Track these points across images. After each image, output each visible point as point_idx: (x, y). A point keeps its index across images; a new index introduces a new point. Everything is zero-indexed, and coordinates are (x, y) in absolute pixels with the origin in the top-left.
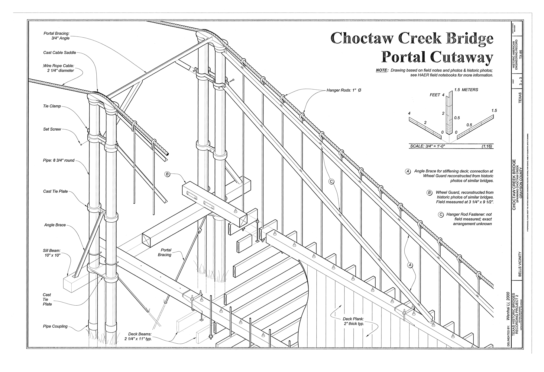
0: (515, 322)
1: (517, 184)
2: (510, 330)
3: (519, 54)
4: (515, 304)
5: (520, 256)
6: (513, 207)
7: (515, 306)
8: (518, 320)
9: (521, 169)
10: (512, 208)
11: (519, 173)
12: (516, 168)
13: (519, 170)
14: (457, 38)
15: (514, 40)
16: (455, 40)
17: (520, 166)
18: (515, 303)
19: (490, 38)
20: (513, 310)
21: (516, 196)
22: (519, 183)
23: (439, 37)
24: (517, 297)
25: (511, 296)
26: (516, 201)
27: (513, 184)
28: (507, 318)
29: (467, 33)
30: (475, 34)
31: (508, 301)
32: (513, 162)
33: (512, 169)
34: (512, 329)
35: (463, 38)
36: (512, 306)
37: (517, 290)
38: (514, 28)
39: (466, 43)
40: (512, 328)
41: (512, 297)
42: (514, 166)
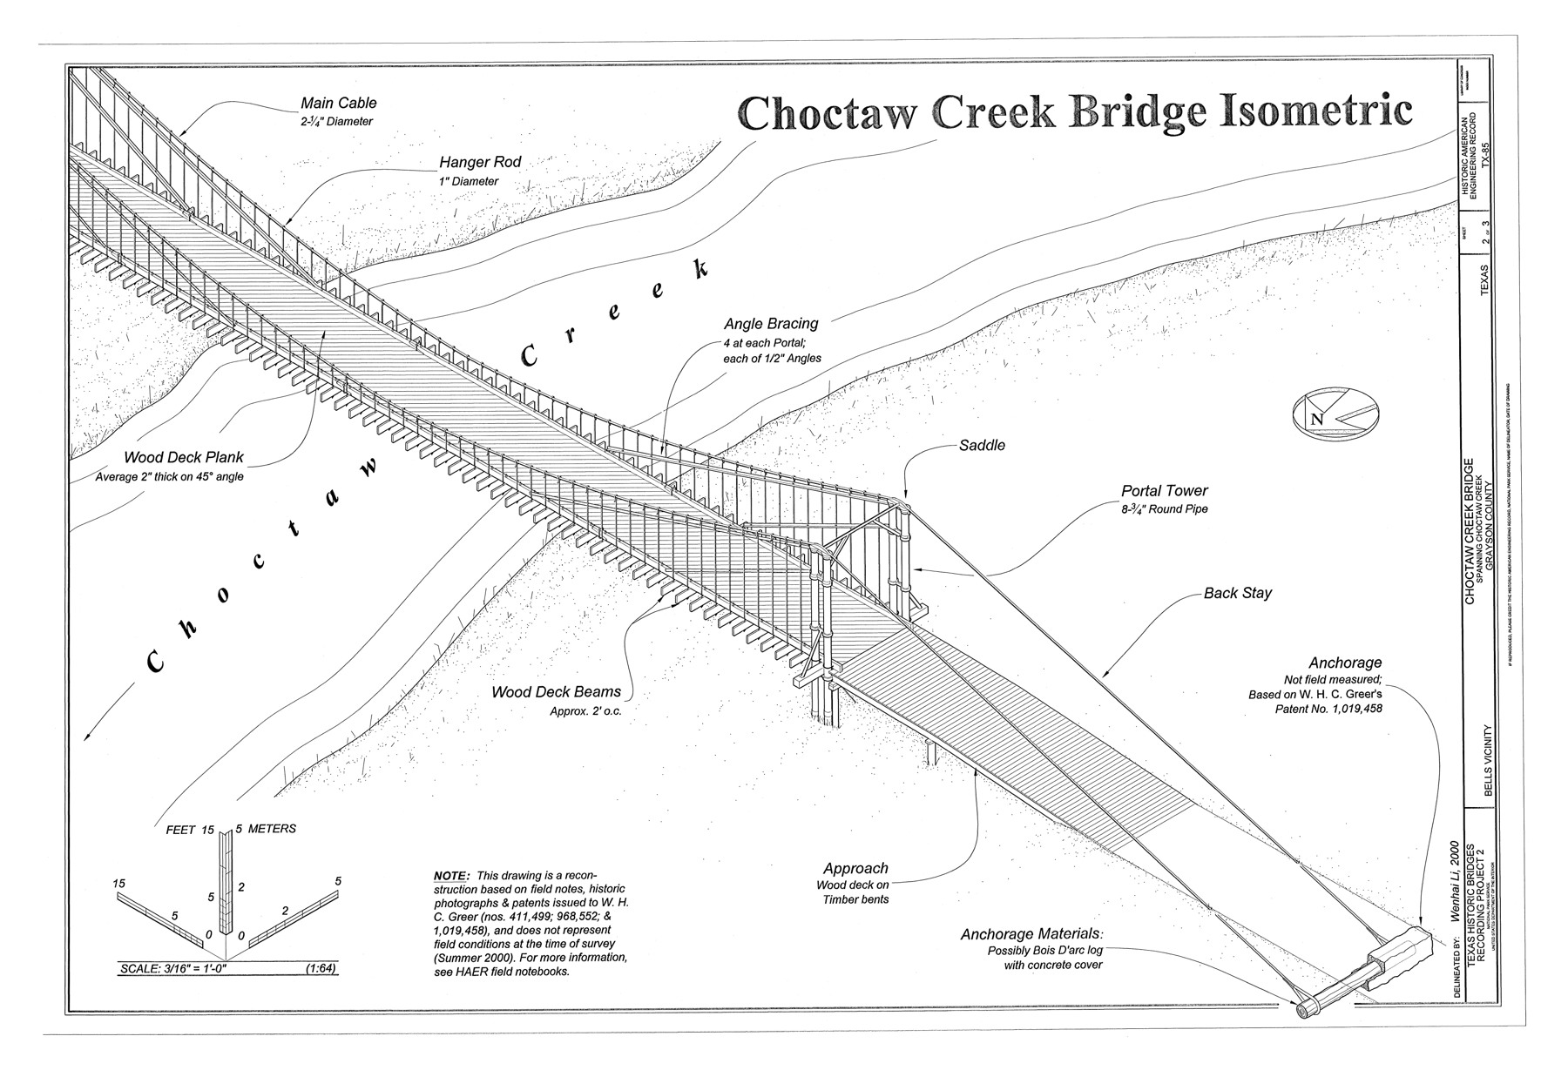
0: (1476, 928)
1: (1479, 528)
2: (1461, 950)
3: (1480, 155)
4: (1475, 876)
5: (1487, 736)
6: (1467, 597)
7: (1476, 880)
8: (1485, 921)
9: (1490, 487)
10: (1465, 597)
11: (1484, 496)
12: (1474, 482)
13: (1483, 489)
14: (1100, 111)
15: (1465, 111)
16: (1094, 116)
17: (1487, 477)
18: (1475, 873)
19: (1197, 109)
20: (1471, 892)
21: (1475, 565)
22: (1484, 526)
23: (1048, 107)
24: (1480, 856)
25: (1462, 853)
26: (1474, 579)
27: (1466, 529)
28: (1453, 916)
29: (1386, 95)
30: (1154, 97)
31: (1455, 868)
32: (1466, 465)
33: (1464, 486)
34: (1467, 948)
35: (1376, 107)
36: (1467, 880)
37: (1480, 836)
38: (1464, 80)
39: (1127, 125)
40: (1468, 943)
41: (1466, 857)
42: (1469, 478)
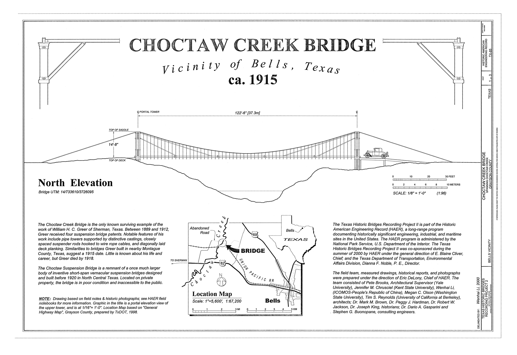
0: (485, 306)
1: (487, 175)
2: (480, 313)
3: (488, 53)
4: (485, 289)
5: (489, 243)
6: (483, 197)
7: (485, 290)
8: (488, 304)
9: (491, 161)
10: (482, 198)
11: (489, 164)
12: (485, 160)
13: (489, 162)
15: (484, 38)
20: (483, 294)
21: (486, 187)
22: (489, 174)
24: (486, 282)
25: (481, 281)
26: (485, 192)
27: (483, 175)
28: (477, 302)
31: (478, 286)
32: (483, 154)
34: (482, 312)
36: (482, 290)
37: (487, 275)
40: (482, 311)
41: (482, 283)
42: (484, 158)
